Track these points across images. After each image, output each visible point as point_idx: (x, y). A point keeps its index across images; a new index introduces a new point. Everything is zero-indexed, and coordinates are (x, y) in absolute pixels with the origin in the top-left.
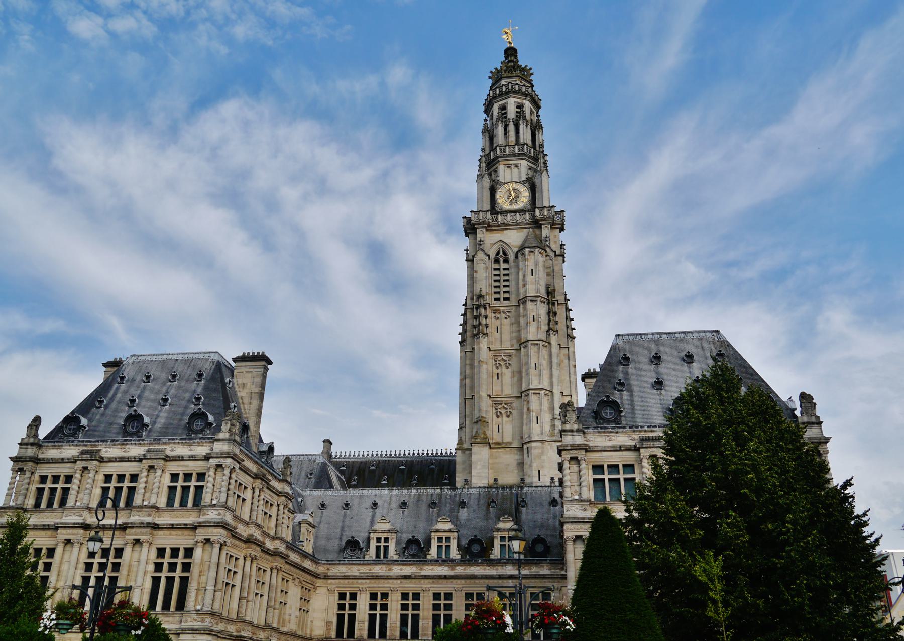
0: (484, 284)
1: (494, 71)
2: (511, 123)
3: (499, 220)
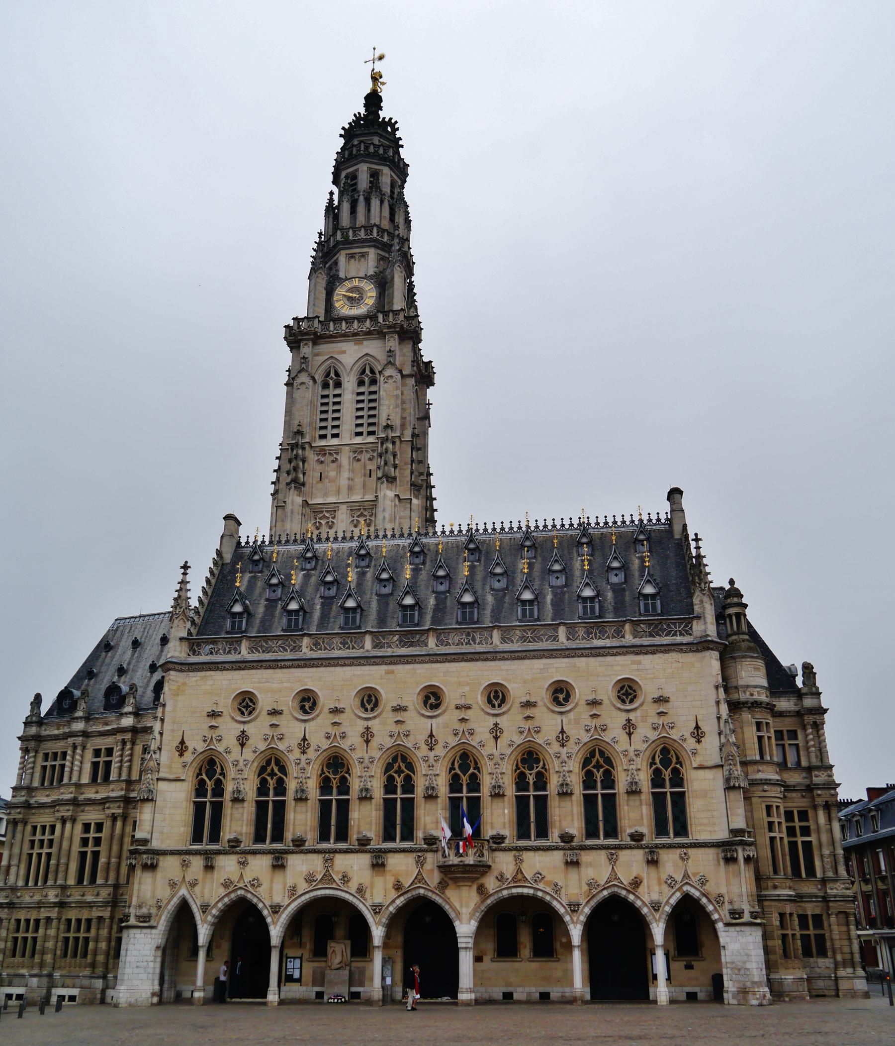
0: (306, 416)
1: (347, 126)
2: (361, 198)
3: (332, 328)
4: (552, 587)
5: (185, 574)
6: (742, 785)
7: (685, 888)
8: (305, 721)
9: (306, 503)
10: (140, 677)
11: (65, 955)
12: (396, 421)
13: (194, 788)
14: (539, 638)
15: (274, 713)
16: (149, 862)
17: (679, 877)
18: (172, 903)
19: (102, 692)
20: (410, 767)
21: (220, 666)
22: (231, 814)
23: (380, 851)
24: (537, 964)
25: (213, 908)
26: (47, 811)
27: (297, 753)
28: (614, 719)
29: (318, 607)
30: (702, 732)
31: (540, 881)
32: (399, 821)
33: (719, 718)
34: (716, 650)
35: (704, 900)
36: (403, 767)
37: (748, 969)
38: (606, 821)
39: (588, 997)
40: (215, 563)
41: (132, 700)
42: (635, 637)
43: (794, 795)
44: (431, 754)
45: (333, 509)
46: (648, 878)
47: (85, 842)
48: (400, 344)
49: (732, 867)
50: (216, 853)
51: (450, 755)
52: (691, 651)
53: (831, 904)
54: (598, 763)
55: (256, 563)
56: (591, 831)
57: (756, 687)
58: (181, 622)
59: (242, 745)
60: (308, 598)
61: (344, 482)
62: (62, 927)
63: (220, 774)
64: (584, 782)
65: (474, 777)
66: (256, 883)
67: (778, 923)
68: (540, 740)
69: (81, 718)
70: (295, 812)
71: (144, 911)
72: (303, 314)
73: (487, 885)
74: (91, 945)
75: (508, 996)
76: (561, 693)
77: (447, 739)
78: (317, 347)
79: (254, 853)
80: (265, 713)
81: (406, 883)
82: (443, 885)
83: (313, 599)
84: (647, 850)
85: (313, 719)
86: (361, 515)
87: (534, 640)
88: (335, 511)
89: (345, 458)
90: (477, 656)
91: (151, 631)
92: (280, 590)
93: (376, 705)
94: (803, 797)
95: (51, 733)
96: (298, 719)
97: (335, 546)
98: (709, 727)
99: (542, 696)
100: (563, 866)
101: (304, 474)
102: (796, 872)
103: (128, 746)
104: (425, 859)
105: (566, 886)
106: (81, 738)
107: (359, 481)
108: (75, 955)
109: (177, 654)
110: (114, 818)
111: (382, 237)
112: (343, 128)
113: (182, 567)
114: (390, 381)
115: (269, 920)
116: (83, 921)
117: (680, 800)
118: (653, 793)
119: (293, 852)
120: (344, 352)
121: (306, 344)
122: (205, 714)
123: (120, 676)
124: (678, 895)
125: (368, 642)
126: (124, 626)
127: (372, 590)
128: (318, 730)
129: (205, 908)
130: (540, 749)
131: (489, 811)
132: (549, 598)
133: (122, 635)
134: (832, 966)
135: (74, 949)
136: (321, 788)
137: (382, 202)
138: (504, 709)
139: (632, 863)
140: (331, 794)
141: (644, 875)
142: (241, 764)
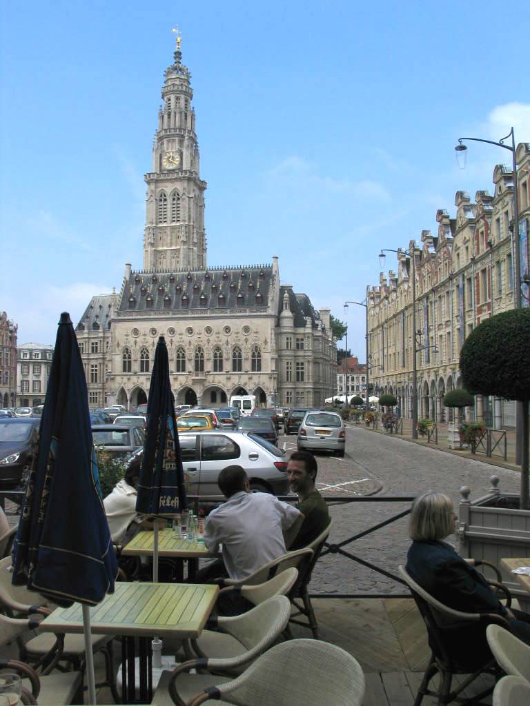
12: (187, 219)
28: (242, 337)
47: (92, 370)
54: (237, 351)
56: (234, 370)
61: (169, 241)
65: (202, 354)
77: (195, 343)
82: (193, 384)
97: (163, 274)
99: (221, 330)
102: (298, 380)
110: (100, 364)
117: (259, 361)
139: (245, 379)
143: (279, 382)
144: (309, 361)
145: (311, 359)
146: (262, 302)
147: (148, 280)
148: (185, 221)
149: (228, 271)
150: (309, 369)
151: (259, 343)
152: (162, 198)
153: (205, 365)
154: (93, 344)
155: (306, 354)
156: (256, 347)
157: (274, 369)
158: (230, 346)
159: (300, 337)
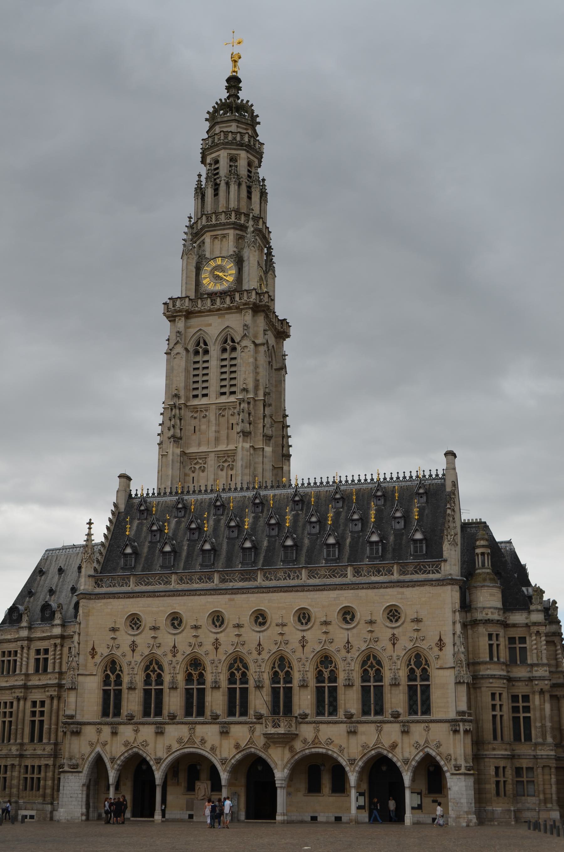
3: (199, 306)
4: (351, 532)
5: (90, 528)
6: (466, 681)
7: (426, 750)
8: (175, 634)
9: (183, 453)
10: (64, 597)
11: (26, 789)
12: (251, 386)
13: (102, 680)
14: (334, 576)
15: (155, 628)
16: (75, 730)
17: (422, 742)
18: (91, 756)
19: (39, 608)
20: (246, 667)
21: (116, 595)
22: (128, 698)
23: (225, 723)
24: (334, 798)
25: (118, 759)
26: (7, 692)
27: (170, 657)
28: (384, 632)
29: (186, 548)
30: (443, 644)
31: (330, 744)
32: (238, 703)
33: (454, 634)
34: (456, 584)
35: (438, 758)
36: (241, 667)
37: (462, 803)
38: (376, 704)
39: (367, 820)
40: (113, 513)
41: (59, 616)
42: (401, 575)
43: (520, 684)
44: (260, 657)
45: (204, 456)
46: (402, 743)
47: (33, 714)
48: (253, 316)
49: (457, 736)
50: (118, 724)
51: (272, 658)
52: (438, 585)
53: (539, 760)
54: (371, 665)
55: (142, 512)
56: (366, 712)
57: (490, 608)
58: (89, 564)
59: (133, 651)
60: (179, 541)
61: (212, 435)
62: (22, 771)
63: (119, 671)
64: (362, 677)
66: (145, 744)
67: (494, 773)
68: (332, 648)
69: (26, 627)
70: (169, 696)
71: (74, 761)
72: (177, 294)
73: (296, 747)
74: (42, 783)
75: (314, 819)
76: (348, 615)
77: (270, 648)
78: (189, 321)
79: (143, 724)
80: (147, 628)
81: (243, 745)
82: (266, 747)
83: (182, 541)
84: (402, 724)
85: (180, 633)
86: (226, 461)
87: (331, 577)
88: (206, 458)
89: (212, 416)
90: (291, 589)
91: (71, 561)
92: (158, 535)
93: (222, 623)
94: (527, 685)
95: (6, 637)
96: (170, 633)
97: (200, 497)
98: (448, 640)
99: (334, 616)
100: (346, 734)
101: (181, 429)
102: (517, 738)
103: (59, 648)
104: (255, 729)
105: (348, 747)
106: (26, 642)
107: (224, 433)
108: (32, 789)
109: (87, 587)
110: (52, 698)
111: (240, 219)
112: (208, 113)
113: (87, 524)
114: (246, 350)
115: (154, 768)
116: (36, 767)
117: (426, 689)
118: (408, 685)
119: (168, 724)
120: (210, 325)
121: (180, 319)
122: (108, 629)
123: (51, 595)
124: (421, 754)
125: (216, 577)
126: (52, 556)
127: (224, 534)
128: (183, 640)
129: (113, 760)
130: (333, 654)
131: (298, 697)
132: (348, 540)
133: (51, 563)
134: (538, 802)
135: (31, 784)
136: (187, 680)
137: (239, 185)
138: (309, 626)
139: (392, 732)
140: (193, 685)
141: (399, 741)
142: (133, 664)
143: (478, 743)
144: (542, 692)
145: (545, 685)
146: (432, 551)
147: (168, 509)
148: (245, 390)
149: (342, 488)
150: (541, 709)
151: (424, 645)
152: (201, 347)
153: (295, 699)
154: (38, 652)
155: (535, 674)
156: (418, 656)
157: (463, 707)
158: (354, 653)
159: (516, 633)
